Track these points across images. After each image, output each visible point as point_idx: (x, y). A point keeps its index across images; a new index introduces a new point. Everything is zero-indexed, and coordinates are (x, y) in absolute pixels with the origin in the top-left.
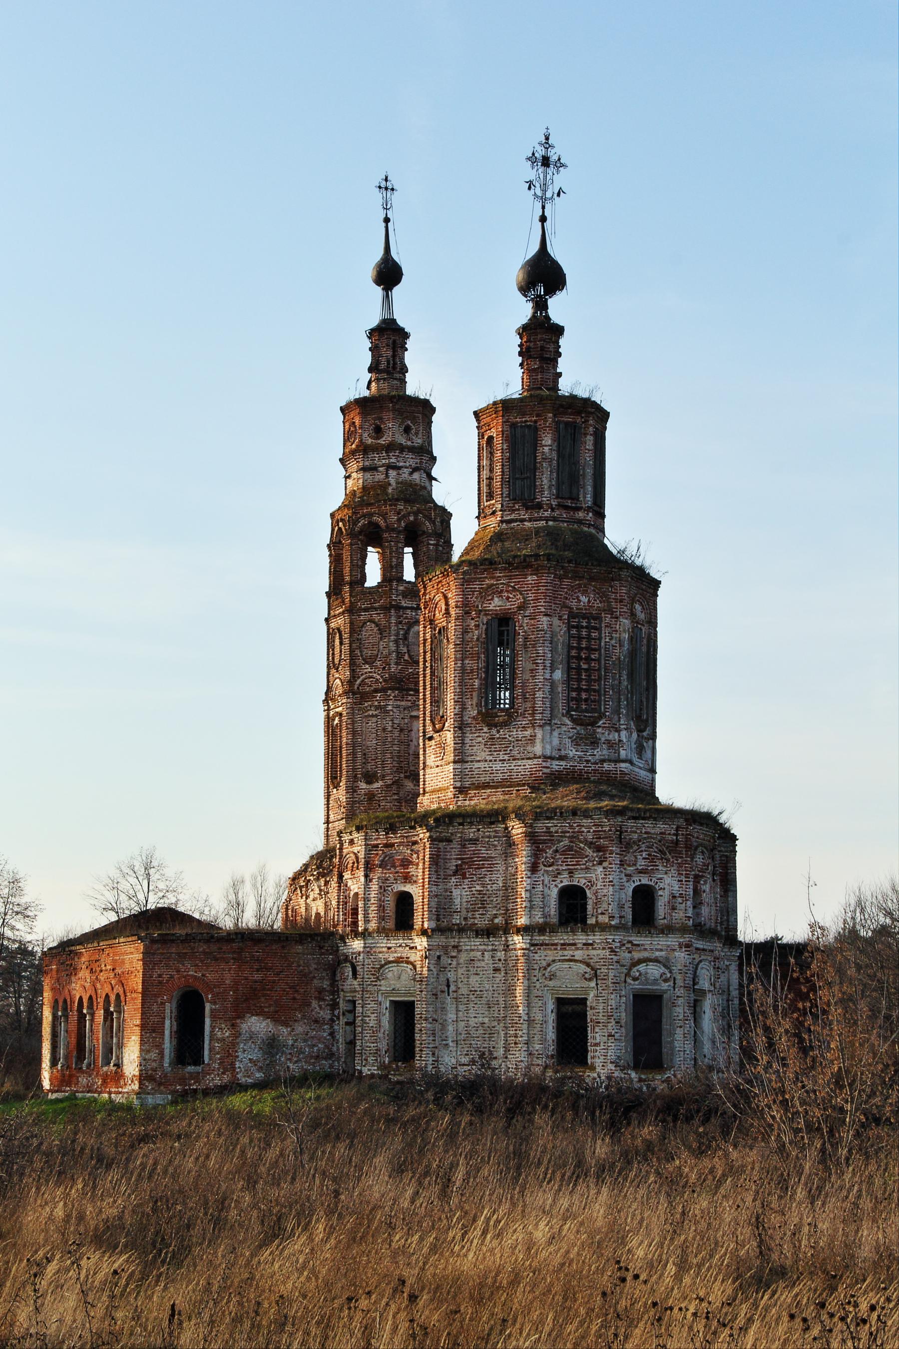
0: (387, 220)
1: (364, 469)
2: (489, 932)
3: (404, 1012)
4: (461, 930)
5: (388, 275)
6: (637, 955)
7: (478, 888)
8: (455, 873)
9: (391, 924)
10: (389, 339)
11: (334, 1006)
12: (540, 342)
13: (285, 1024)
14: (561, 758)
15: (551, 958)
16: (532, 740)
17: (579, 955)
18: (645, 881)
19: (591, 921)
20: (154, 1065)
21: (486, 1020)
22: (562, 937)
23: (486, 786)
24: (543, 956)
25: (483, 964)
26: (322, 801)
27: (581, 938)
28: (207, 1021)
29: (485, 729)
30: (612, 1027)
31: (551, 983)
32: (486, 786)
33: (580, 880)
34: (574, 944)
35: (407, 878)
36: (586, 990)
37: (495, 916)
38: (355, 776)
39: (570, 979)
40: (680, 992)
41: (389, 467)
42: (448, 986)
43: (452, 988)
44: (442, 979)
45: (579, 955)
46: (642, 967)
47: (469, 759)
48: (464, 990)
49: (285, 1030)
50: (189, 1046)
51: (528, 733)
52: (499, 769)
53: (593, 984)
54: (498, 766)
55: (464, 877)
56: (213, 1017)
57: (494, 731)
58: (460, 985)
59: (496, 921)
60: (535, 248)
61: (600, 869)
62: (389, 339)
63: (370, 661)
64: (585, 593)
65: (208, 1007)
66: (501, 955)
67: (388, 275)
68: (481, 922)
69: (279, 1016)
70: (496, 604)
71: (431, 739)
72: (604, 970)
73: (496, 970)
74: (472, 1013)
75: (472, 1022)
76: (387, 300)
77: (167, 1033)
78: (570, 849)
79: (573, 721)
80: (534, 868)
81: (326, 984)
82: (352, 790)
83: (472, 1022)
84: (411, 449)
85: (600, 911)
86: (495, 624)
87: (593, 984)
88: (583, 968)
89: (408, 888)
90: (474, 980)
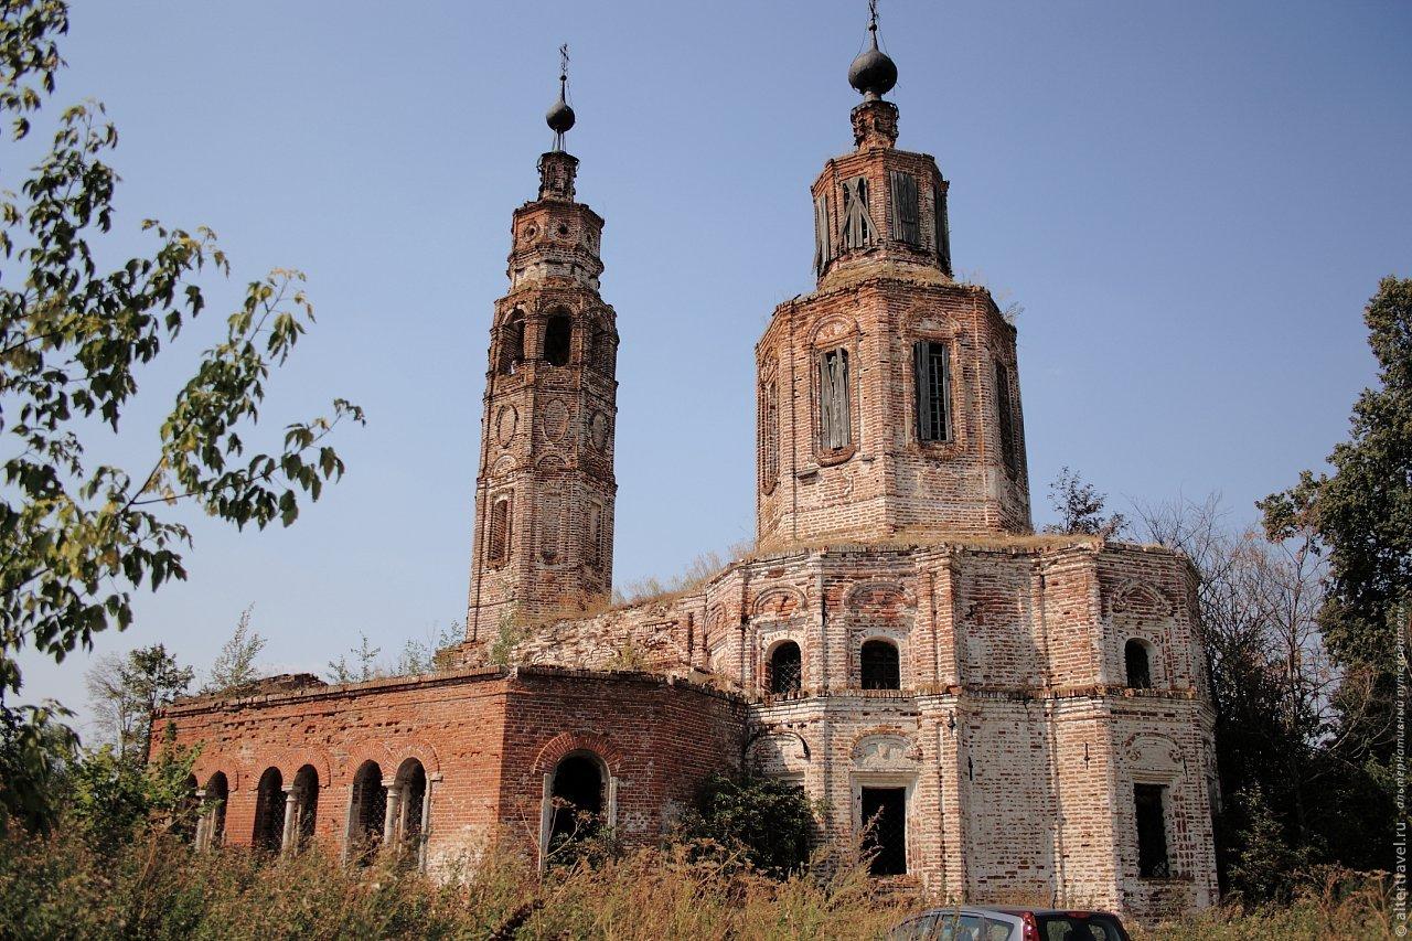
4: (989, 691)
5: (562, 120)
7: (1002, 637)
10: (558, 166)
15: (1132, 731)
17: (1163, 727)
33: (1146, 634)
34: (1155, 714)
38: (532, 555)
41: (575, 264)
42: (971, 766)
43: (976, 770)
47: (902, 493)
48: (992, 773)
53: (1180, 766)
55: (980, 622)
56: (620, 800)
58: (985, 766)
61: (1172, 621)
62: (558, 166)
65: (612, 785)
67: (562, 120)
70: (928, 327)
74: (1006, 805)
75: (1006, 818)
78: (1137, 592)
83: (1006, 818)
85: (1178, 674)
86: (926, 347)
87: (1180, 766)
88: (1171, 746)
90: (1005, 757)
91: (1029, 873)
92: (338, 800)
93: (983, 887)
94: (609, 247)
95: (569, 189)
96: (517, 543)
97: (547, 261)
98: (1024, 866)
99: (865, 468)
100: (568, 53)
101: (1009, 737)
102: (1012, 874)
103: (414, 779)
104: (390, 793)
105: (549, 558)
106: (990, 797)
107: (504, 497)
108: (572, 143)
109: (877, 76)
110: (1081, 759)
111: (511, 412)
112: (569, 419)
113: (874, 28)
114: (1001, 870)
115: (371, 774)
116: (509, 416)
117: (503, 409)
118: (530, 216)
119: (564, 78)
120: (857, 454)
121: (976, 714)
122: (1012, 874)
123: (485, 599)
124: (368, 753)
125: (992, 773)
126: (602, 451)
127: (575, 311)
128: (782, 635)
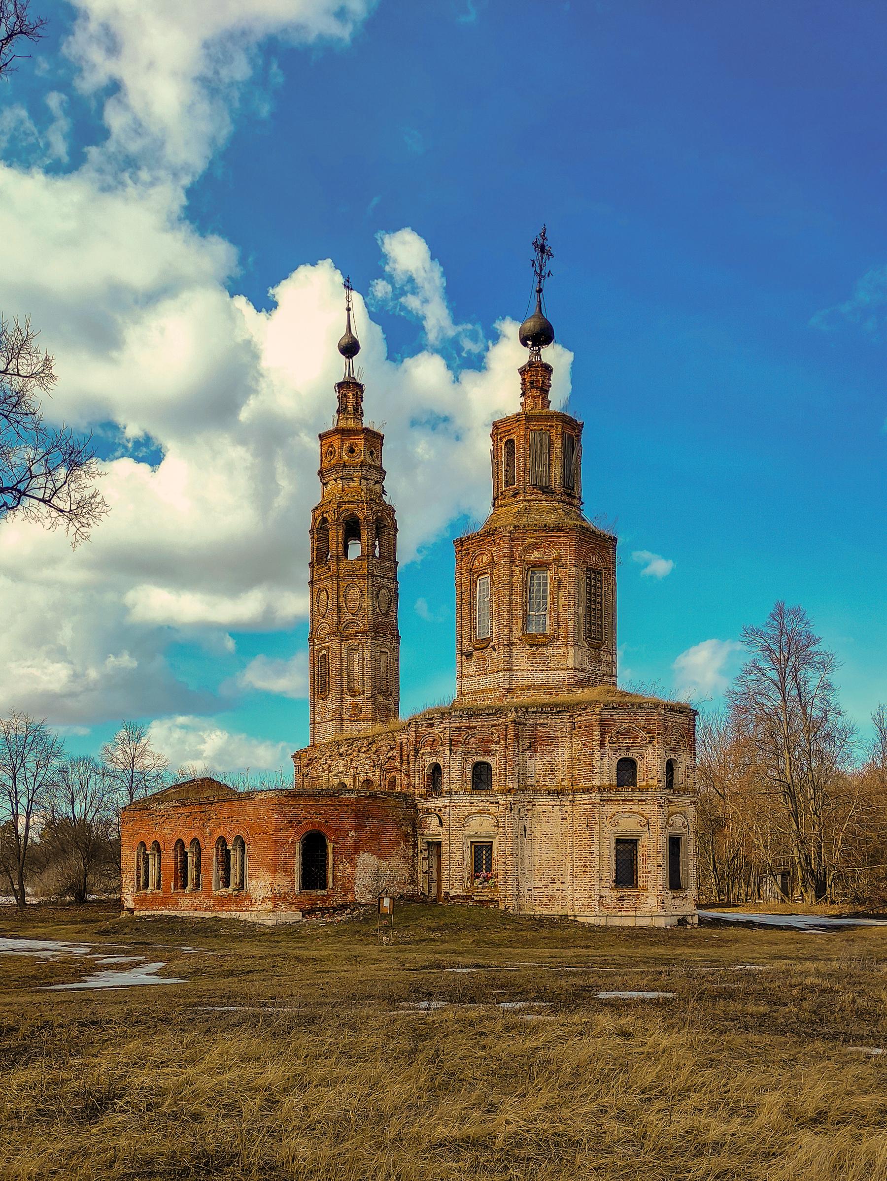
2: (558, 793)
3: (481, 852)
6: (672, 809)
7: (548, 759)
8: (530, 748)
9: (469, 787)
11: (415, 846)
13: (385, 858)
14: (583, 670)
16: (565, 655)
17: (635, 808)
18: (672, 757)
19: (641, 783)
20: (286, 889)
22: (626, 793)
23: (529, 688)
26: (310, 708)
27: (638, 796)
28: (331, 856)
29: (528, 647)
30: (660, 860)
32: (529, 688)
33: (633, 754)
34: (632, 800)
35: (488, 752)
36: (640, 834)
38: (342, 691)
39: (629, 826)
40: (692, 835)
42: (525, 831)
43: (528, 832)
44: (521, 826)
45: (635, 808)
46: (673, 817)
48: (537, 834)
49: (385, 863)
50: (314, 874)
51: (563, 650)
52: (539, 677)
53: (646, 829)
54: (538, 674)
55: (536, 751)
57: (534, 649)
59: (563, 783)
64: (593, 554)
65: (330, 846)
68: (552, 785)
69: (382, 856)
72: (654, 819)
74: (544, 850)
76: (350, 368)
77: (297, 865)
79: (589, 644)
80: (602, 745)
81: (410, 830)
84: (375, 467)
85: (650, 776)
87: (646, 829)
89: (486, 759)
91: (558, 885)
92: (211, 854)
95: (358, 412)
96: (333, 682)
97: (342, 478)
98: (553, 881)
102: (546, 886)
104: (232, 852)
105: (353, 693)
107: (324, 652)
110: (584, 826)
112: (360, 599)
114: (540, 884)
115: (222, 841)
116: (323, 596)
118: (330, 440)
122: (546, 886)
124: (220, 833)
126: (386, 615)
127: (361, 517)
128: (434, 760)
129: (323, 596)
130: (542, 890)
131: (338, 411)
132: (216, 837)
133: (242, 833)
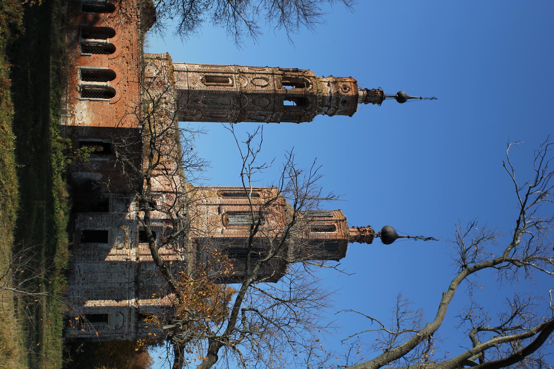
0: (421, 98)
1: (331, 97)
2: (137, 282)
5: (401, 98)
12: (365, 238)
15: (125, 314)
17: (126, 323)
20: (80, 133)
21: (99, 280)
24: (126, 313)
25: (123, 278)
27: (133, 325)
28: (101, 159)
31: (114, 315)
34: (130, 321)
37: (143, 283)
43: (113, 266)
45: (126, 323)
56: (102, 162)
59: (141, 284)
60: (400, 235)
63: (253, 102)
66: (127, 286)
67: (401, 98)
68: (140, 278)
71: (220, 212)
73: (120, 284)
82: (200, 92)
87: (114, 328)
91: (81, 281)
93: (77, 267)
94: (340, 119)
98: (83, 279)
99: (220, 230)
100: (433, 100)
101: (123, 276)
103: (109, 93)
106: (105, 270)
107: (231, 82)
108: (389, 104)
109: (387, 238)
111: (266, 83)
113: (409, 237)
114: (82, 272)
116: (264, 83)
117: (267, 80)
118: (353, 88)
119: (421, 98)
120: (225, 228)
121: (131, 266)
123: (190, 75)
125: (112, 271)
126: (250, 118)
129: (264, 83)
130: (78, 274)
131: (368, 90)
132: (116, 70)
133: (117, 96)
